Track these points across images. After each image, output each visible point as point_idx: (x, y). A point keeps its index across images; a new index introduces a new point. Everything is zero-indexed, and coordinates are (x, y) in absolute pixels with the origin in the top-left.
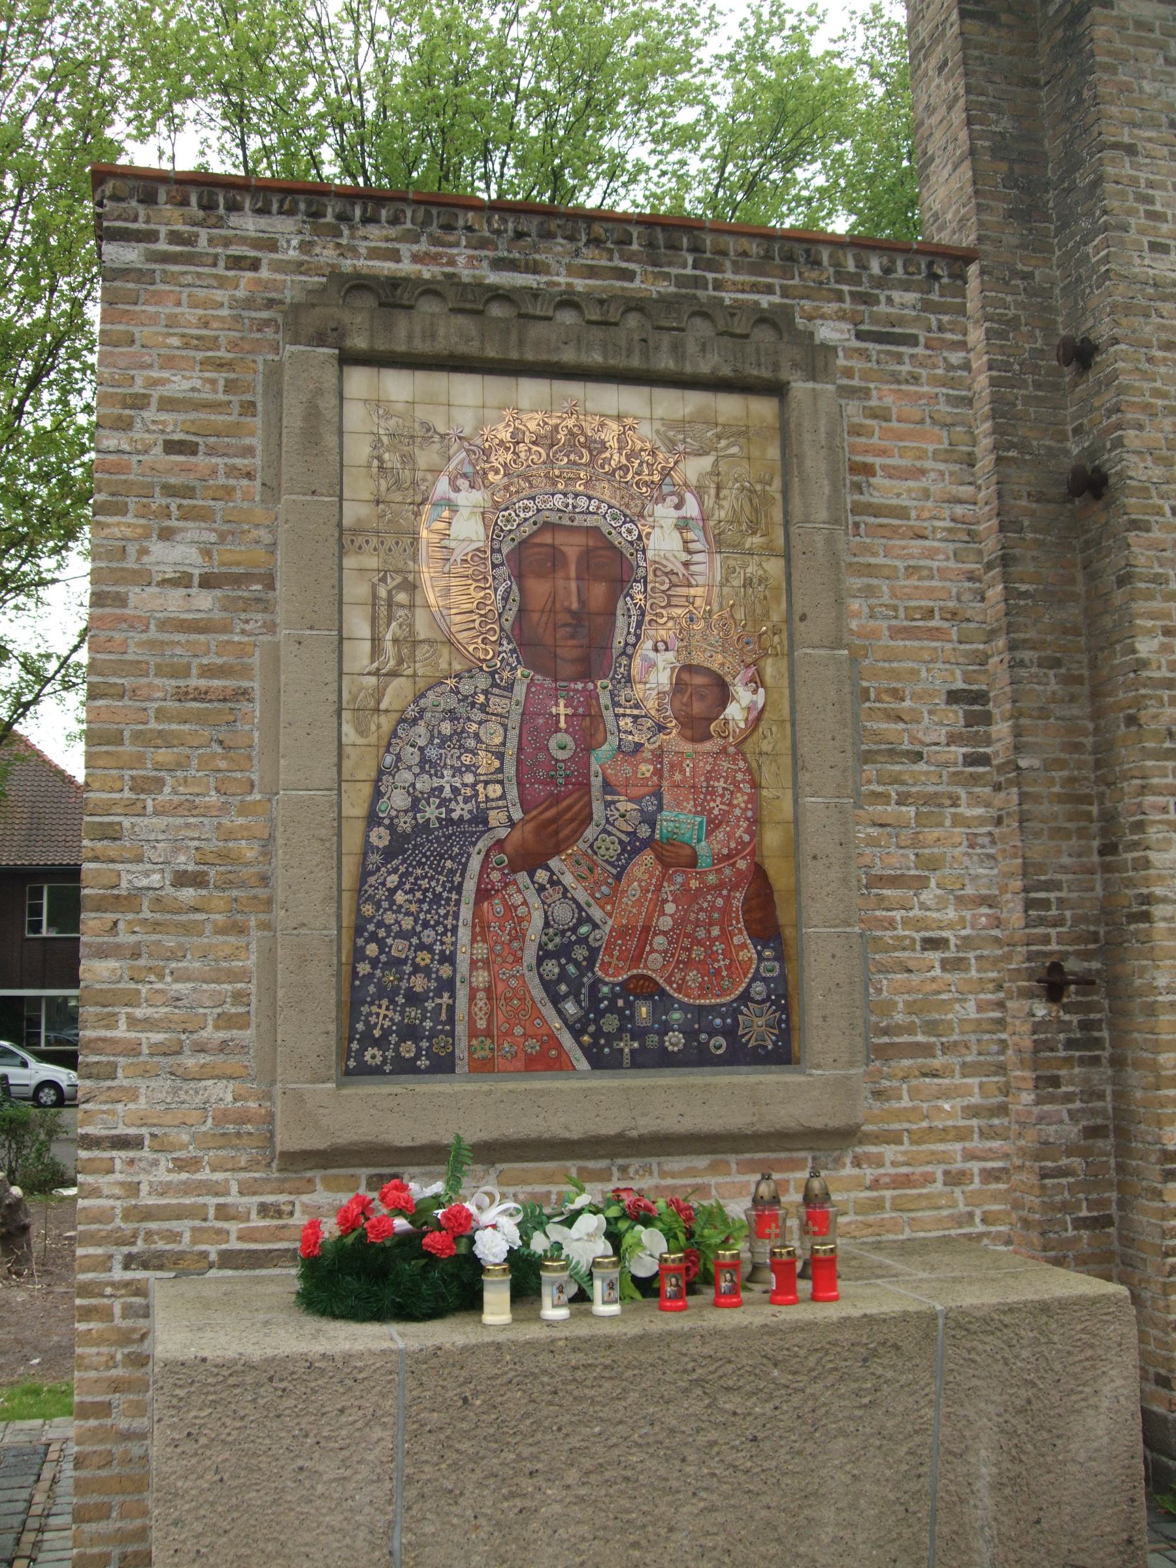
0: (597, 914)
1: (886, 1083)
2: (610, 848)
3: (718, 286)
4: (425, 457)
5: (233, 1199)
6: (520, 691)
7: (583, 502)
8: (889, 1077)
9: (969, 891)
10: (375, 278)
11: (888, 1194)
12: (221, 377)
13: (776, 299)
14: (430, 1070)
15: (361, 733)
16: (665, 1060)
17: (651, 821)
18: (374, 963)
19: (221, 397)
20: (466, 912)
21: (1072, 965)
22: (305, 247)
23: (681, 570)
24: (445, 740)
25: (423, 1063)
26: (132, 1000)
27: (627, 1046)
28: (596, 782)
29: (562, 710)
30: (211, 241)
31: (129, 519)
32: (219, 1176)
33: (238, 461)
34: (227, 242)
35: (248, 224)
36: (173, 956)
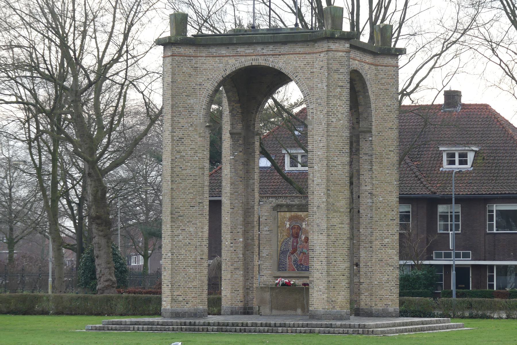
2: (299, 253)
16: (303, 270)
22: (275, 201)
27: (300, 269)
29: (295, 241)
35: (271, 199)
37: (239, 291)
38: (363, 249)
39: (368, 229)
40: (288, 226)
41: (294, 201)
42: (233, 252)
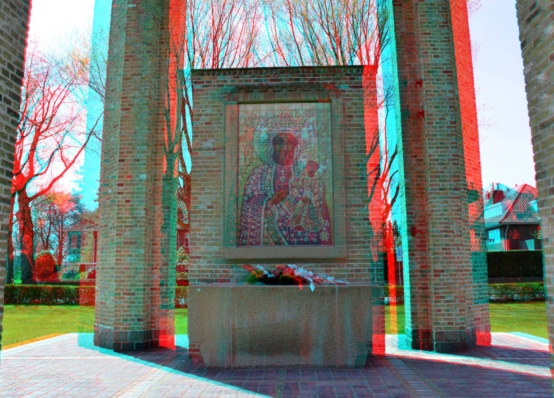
0: (290, 213)
1: (354, 249)
3: (319, 79)
4: (256, 122)
5: (218, 269)
6: (274, 167)
7: (288, 128)
8: (356, 248)
9: (375, 208)
10: (244, 86)
11: (355, 273)
12: (216, 109)
13: (331, 81)
14: (255, 244)
15: (242, 178)
16: (304, 243)
17: (301, 193)
18: (245, 223)
19: (216, 113)
20: (263, 213)
21: (418, 228)
22: (232, 81)
23: (308, 141)
24: (258, 178)
25: (254, 243)
26: (199, 230)
27: (296, 240)
28: (290, 186)
30: (214, 82)
31: (199, 138)
32: (215, 264)
33: (219, 125)
34: (217, 82)
35: (221, 78)
36: (208, 221)
37: (134, 294)
38: (439, 194)
39: (448, 147)
40: (264, 136)
41: (278, 80)
42: (124, 206)
